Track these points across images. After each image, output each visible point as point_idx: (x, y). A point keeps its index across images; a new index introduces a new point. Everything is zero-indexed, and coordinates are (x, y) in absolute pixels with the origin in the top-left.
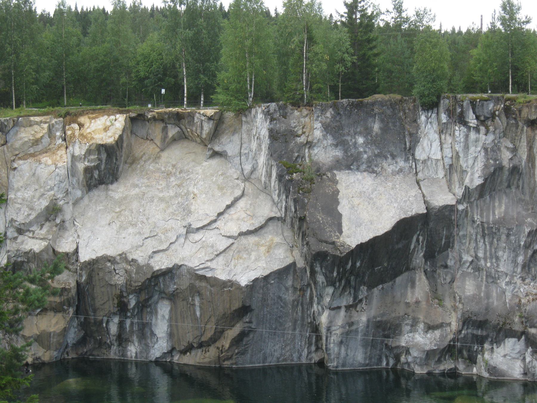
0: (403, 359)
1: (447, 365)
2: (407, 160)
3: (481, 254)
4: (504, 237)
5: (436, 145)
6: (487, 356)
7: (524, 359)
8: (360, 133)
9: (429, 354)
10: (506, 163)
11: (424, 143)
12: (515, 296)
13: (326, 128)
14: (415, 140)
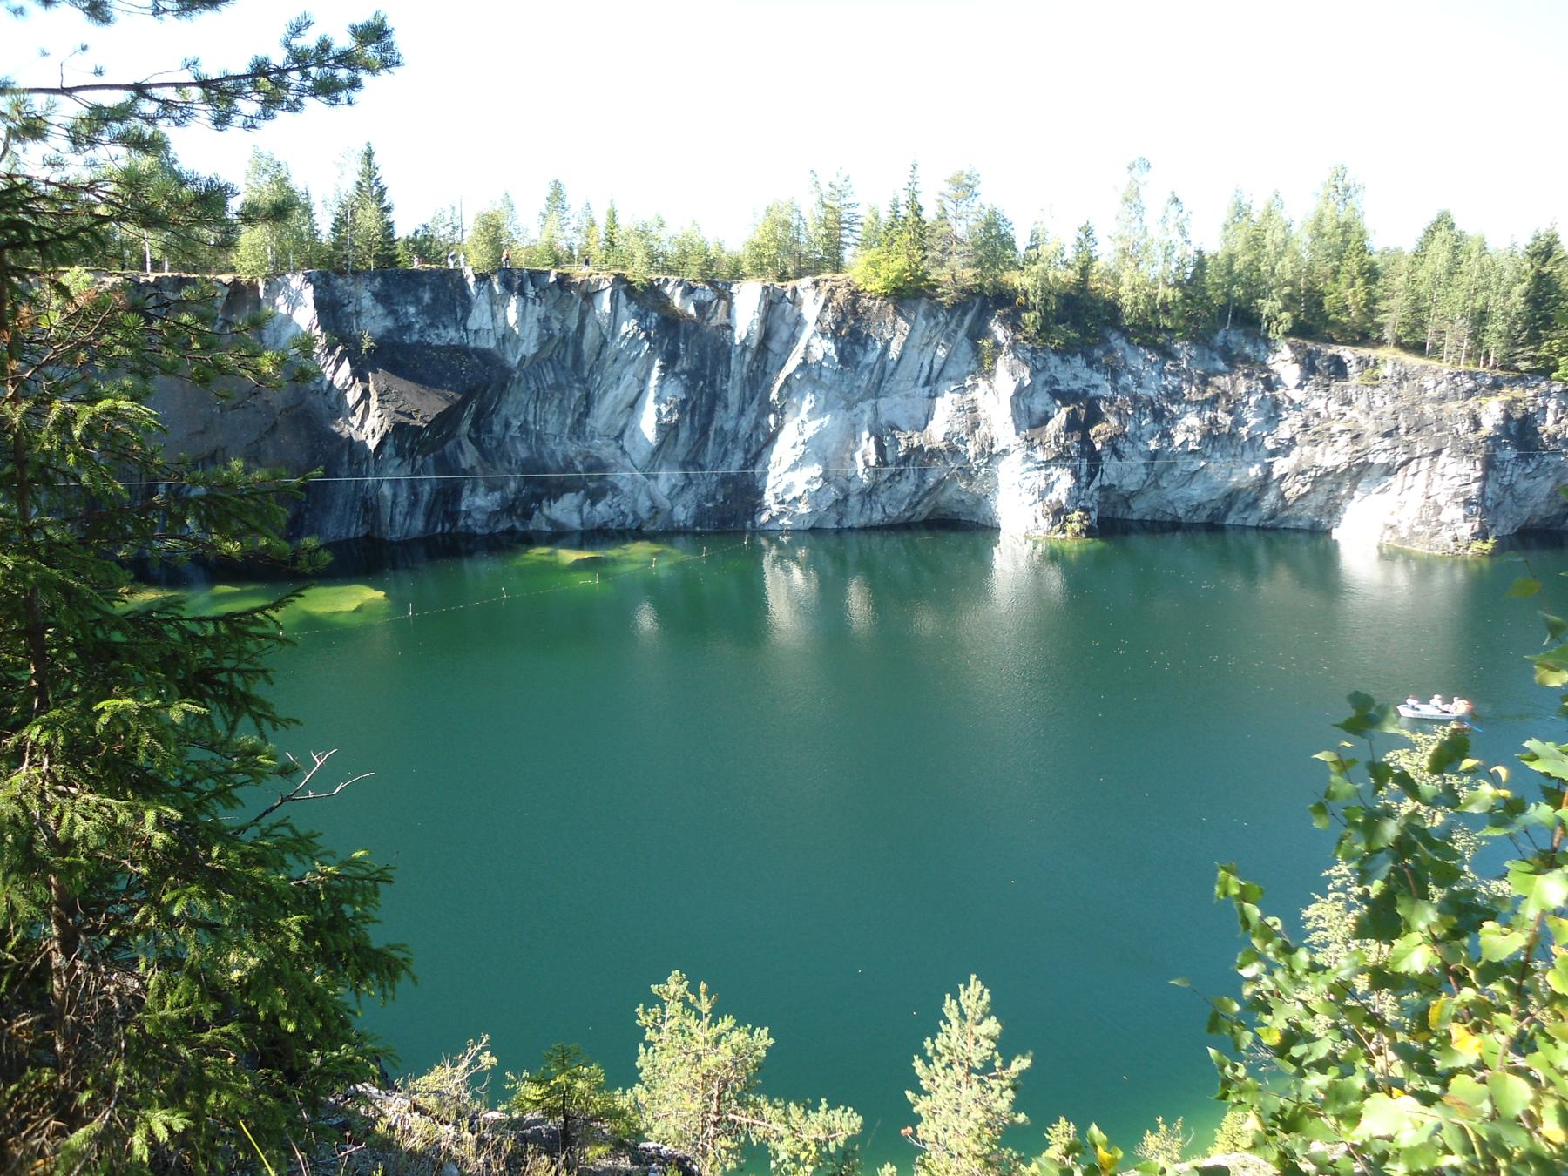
0: (461, 522)
1: (504, 525)
2: (457, 330)
3: (530, 418)
4: (556, 402)
5: (487, 315)
6: (546, 511)
7: (581, 512)
8: (411, 303)
9: (492, 514)
10: (556, 332)
11: (475, 312)
12: (565, 457)
13: (376, 295)
14: (467, 310)
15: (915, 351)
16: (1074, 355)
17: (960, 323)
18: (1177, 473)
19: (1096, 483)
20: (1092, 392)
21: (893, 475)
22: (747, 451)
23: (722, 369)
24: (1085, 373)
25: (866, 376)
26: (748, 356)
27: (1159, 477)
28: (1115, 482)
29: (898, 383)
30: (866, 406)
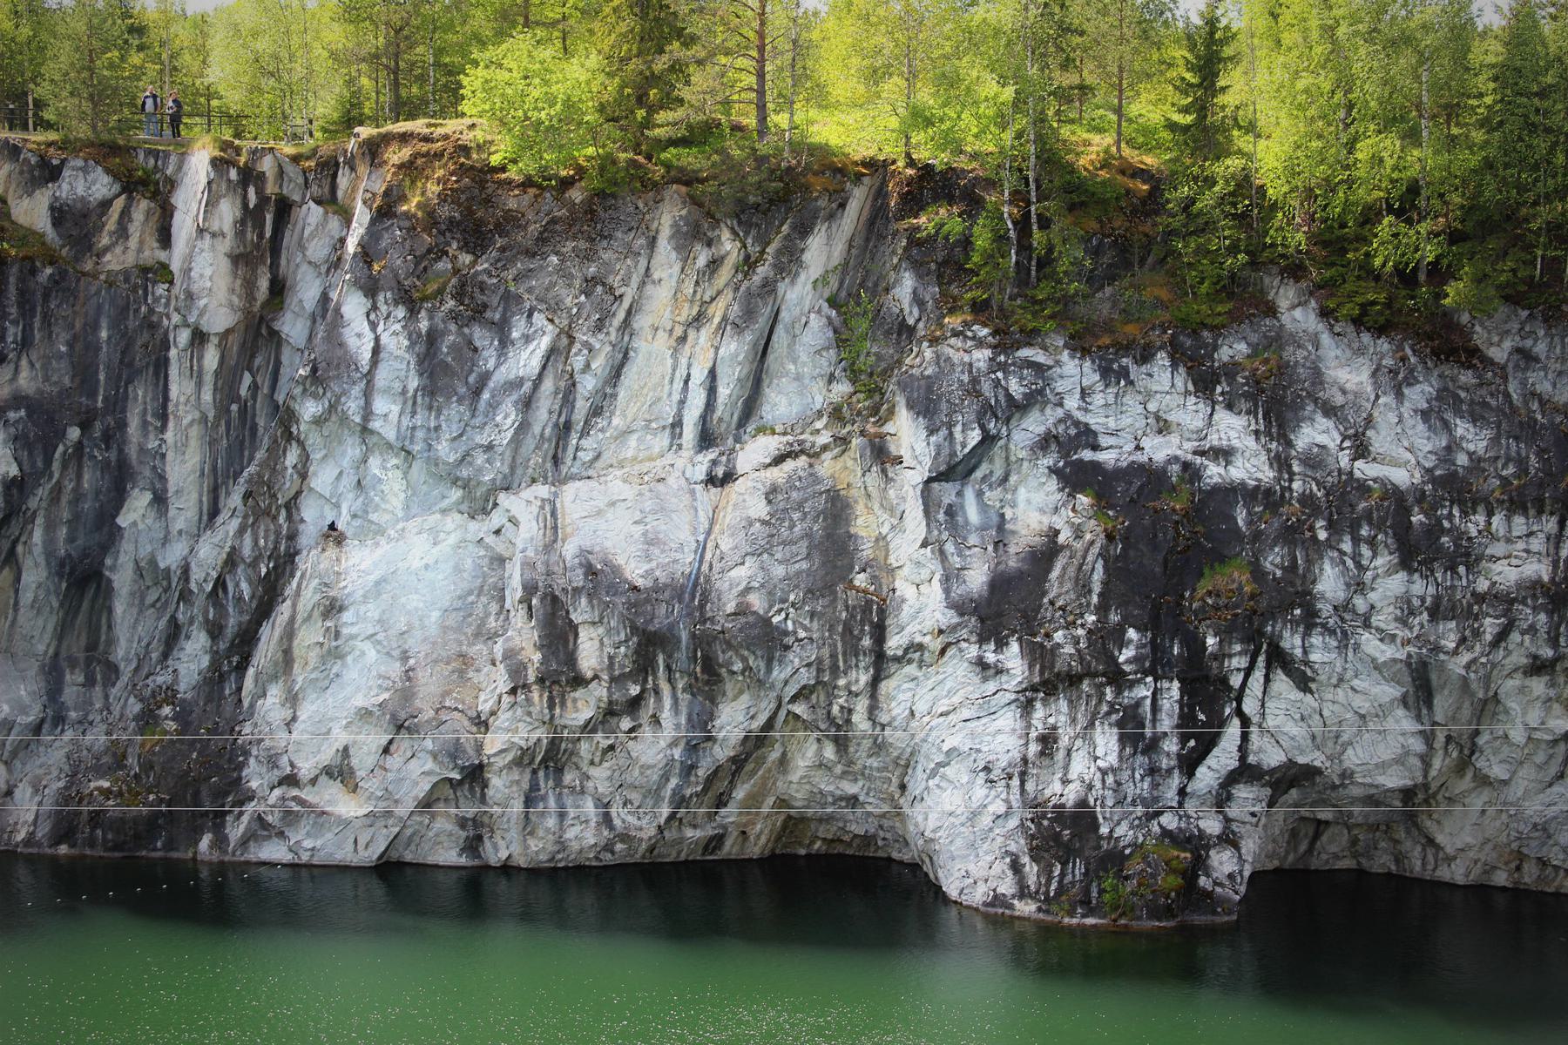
15: (662, 343)
16: (1145, 357)
17: (790, 262)
18: (1518, 735)
19: (1223, 757)
20: (1214, 472)
21: (610, 712)
22: (215, 631)
23: (141, 393)
24: (1189, 413)
25: (508, 417)
26: (211, 358)
27: (1466, 753)
28: (1317, 759)
29: (628, 432)
30: (522, 506)
